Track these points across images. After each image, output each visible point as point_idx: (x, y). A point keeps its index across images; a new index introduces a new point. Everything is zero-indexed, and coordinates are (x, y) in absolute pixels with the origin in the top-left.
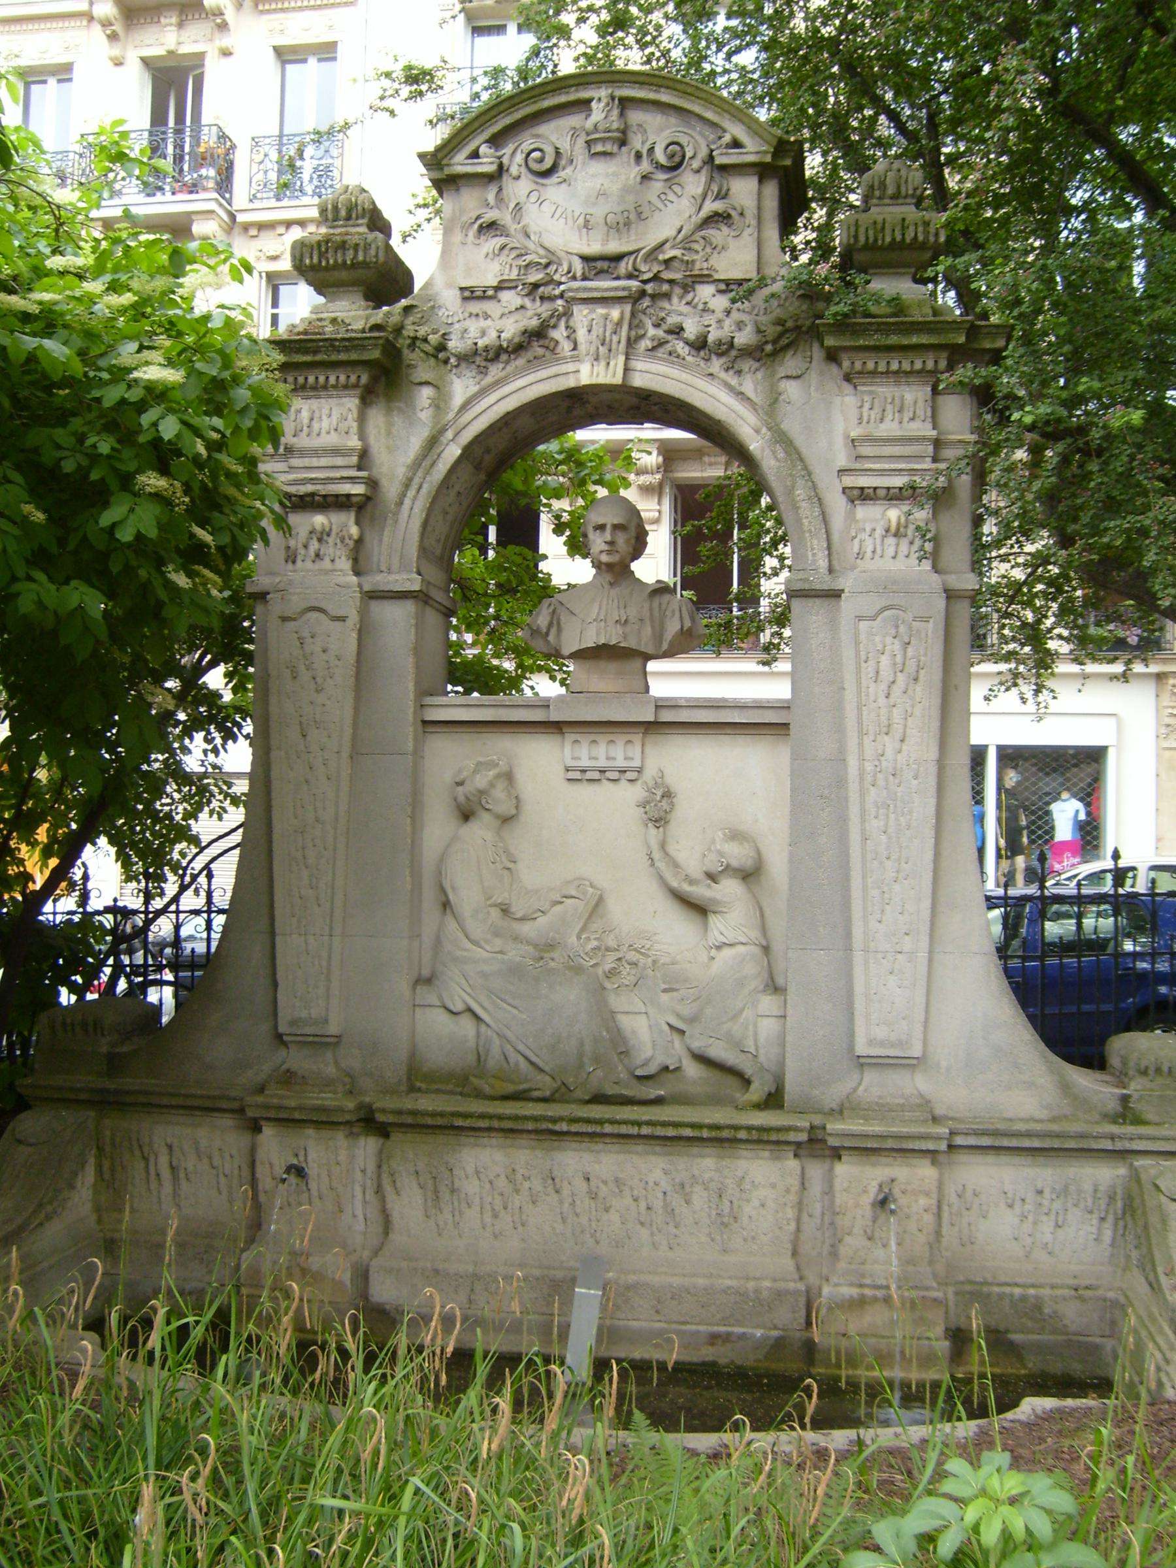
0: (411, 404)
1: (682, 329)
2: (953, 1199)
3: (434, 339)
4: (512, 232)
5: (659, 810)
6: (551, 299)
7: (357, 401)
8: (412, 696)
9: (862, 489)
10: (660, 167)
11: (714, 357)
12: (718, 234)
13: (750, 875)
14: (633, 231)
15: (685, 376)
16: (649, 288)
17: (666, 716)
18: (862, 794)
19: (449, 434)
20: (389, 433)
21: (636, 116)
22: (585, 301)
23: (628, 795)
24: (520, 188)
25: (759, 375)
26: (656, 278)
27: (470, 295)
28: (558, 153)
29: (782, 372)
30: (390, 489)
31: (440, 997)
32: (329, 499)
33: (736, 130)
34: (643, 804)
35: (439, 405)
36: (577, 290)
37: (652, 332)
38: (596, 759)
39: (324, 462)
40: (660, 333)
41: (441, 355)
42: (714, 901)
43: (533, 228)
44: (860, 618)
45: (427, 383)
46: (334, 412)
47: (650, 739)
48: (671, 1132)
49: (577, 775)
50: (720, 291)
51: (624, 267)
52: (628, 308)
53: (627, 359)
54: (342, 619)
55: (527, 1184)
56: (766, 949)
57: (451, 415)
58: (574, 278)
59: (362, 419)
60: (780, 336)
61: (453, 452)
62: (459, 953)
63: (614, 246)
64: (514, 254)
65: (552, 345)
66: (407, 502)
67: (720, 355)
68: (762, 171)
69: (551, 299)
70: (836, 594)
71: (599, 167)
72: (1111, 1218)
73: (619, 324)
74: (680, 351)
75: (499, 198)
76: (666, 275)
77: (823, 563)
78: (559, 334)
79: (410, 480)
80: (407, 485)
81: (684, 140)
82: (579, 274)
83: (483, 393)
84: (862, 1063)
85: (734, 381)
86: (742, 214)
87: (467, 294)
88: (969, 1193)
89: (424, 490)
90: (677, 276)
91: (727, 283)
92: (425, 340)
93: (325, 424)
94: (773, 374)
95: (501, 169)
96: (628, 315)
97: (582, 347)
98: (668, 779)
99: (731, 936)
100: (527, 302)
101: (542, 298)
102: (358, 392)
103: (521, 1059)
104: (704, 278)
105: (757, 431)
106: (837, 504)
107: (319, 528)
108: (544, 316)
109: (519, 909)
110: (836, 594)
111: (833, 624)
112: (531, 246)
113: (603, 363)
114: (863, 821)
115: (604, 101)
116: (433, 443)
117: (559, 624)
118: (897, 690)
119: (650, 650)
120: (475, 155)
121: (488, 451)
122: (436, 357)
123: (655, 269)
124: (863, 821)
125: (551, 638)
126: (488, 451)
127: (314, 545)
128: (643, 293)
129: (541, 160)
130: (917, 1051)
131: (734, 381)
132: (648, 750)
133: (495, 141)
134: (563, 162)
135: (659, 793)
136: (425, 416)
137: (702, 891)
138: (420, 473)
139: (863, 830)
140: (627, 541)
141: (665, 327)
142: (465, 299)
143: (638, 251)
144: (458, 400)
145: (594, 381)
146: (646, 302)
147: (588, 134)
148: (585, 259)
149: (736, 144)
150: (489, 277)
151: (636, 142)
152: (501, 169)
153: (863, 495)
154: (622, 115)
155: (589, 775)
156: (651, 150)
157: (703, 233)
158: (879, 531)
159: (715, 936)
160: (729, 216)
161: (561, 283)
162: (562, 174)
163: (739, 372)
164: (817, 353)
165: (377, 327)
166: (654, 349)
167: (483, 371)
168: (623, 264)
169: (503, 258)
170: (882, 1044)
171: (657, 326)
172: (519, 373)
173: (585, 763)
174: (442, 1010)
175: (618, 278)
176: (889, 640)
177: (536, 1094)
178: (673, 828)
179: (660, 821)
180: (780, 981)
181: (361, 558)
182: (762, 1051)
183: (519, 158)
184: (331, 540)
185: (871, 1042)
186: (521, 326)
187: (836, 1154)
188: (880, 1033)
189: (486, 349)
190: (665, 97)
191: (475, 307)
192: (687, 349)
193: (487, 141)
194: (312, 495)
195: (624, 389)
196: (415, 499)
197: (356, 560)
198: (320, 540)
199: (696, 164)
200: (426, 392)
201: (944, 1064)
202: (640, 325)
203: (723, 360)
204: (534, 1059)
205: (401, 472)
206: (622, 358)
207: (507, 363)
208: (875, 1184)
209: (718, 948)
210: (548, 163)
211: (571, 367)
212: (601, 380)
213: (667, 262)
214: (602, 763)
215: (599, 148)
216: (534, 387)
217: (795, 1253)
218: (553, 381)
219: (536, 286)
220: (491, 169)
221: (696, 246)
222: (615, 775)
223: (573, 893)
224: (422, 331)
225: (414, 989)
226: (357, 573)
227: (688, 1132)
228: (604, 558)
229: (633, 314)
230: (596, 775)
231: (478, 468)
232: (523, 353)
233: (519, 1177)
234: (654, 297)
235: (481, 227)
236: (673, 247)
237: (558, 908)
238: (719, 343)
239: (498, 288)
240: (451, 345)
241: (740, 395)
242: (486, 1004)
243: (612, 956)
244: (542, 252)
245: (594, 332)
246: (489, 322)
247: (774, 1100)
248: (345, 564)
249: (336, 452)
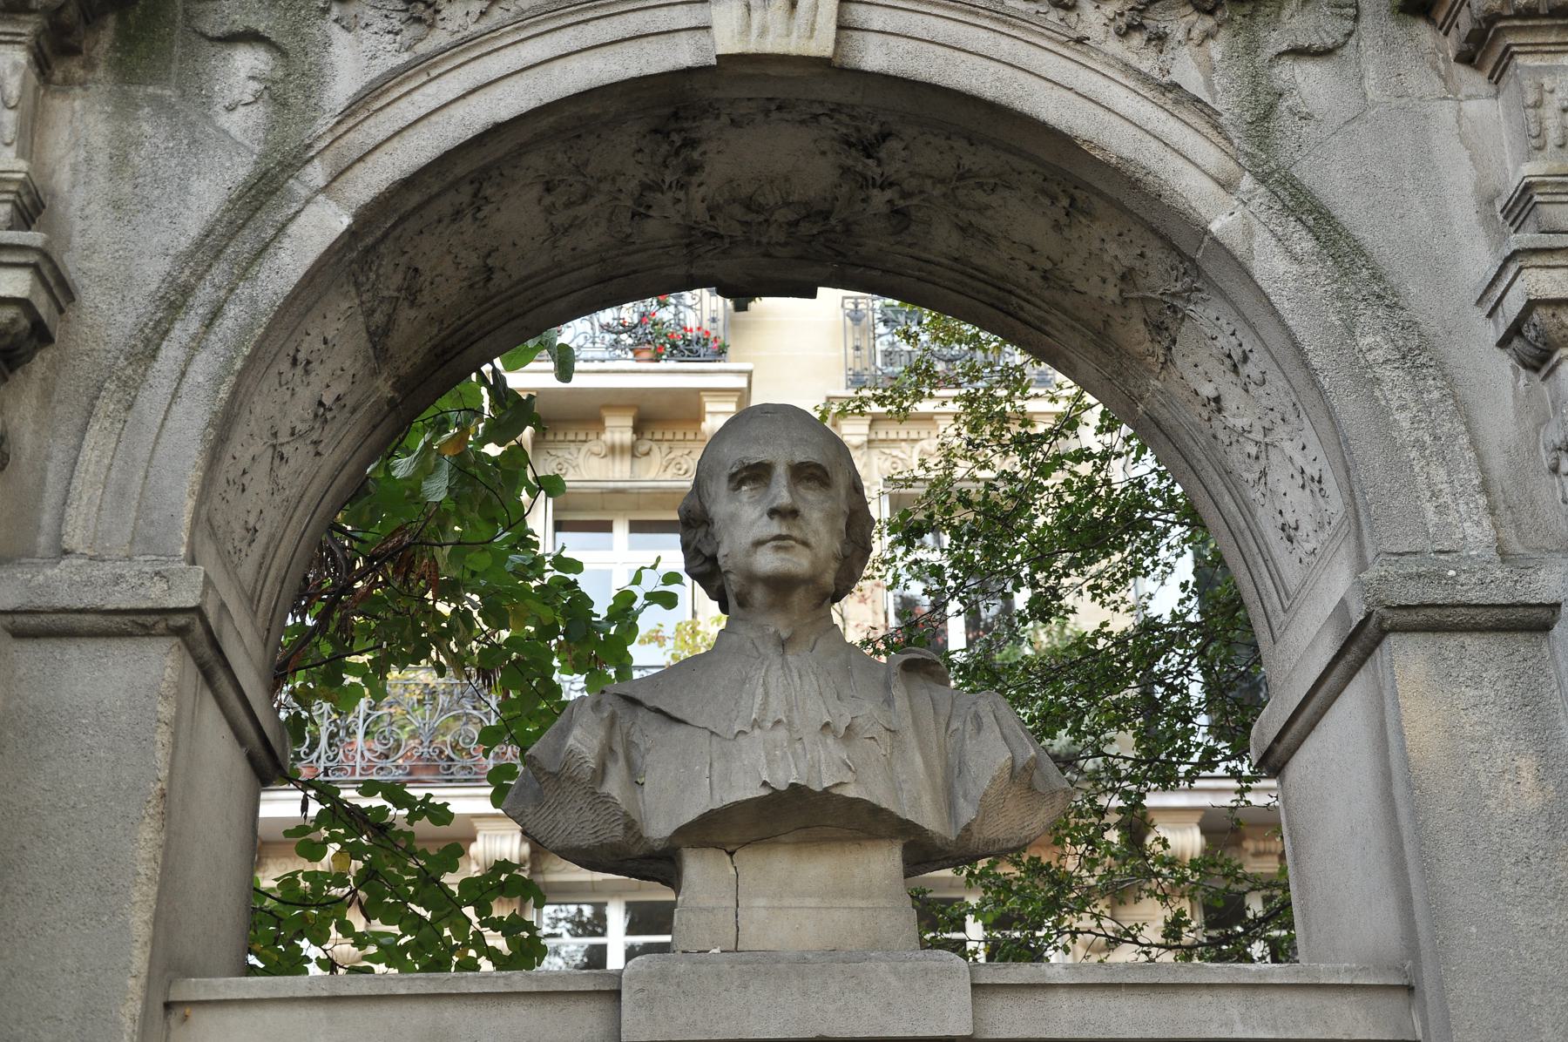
0: (198, 95)
7: (20, 56)
19: (316, 173)
20: (120, 162)
25: (1216, 49)
29: (1277, 41)
30: (108, 314)
35: (286, 95)
45: (251, 37)
57: (323, 124)
61: (321, 224)
66: (171, 353)
79: (187, 291)
80: (174, 301)
83: (422, 67)
85: (1148, 63)
94: (1252, 48)
105: (1227, 185)
110: (1533, 621)
116: (263, 193)
117: (629, 745)
125: (614, 786)
131: (1148, 63)
138: (219, 273)
140: (831, 518)
144: (343, 86)
145: (753, 46)
163: (1159, 39)
196: (199, 341)
200: (247, 62)
205: (154, 271)
216: (574, 63)
228: (768, 562)
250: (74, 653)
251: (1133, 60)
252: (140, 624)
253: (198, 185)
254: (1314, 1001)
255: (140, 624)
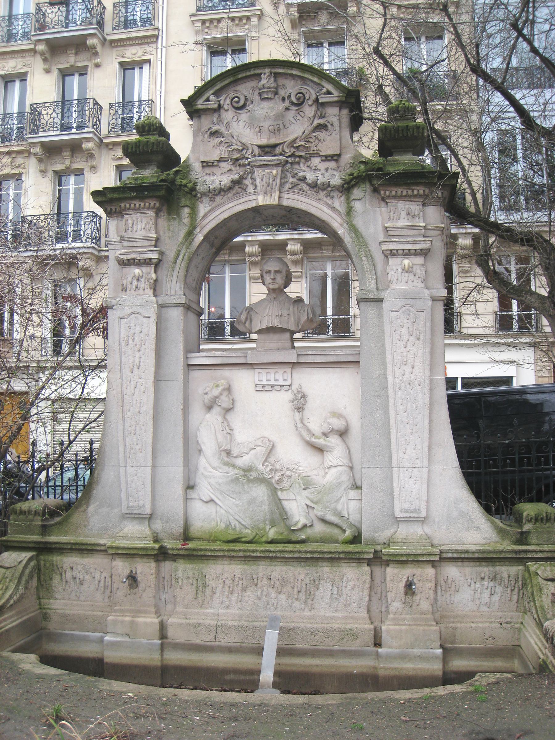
1: (305, 178)
2: (442, 583)
3: (190, 185)
4: (225, 135)
5: (300, 404)
6: (245, 165)
8: (182, 353)
9: (391, 250)
10: (293, 103)
11: (320, 191)
12: (322, 135)
13: (343, 433)
14: (281, 134)
15: (307, 200)
16: (289, 160)
17: (302, 360)
18: (395, 394)
19: (198, 230)
21: (281, 81)
22: (260, 166)
23: (285, 397)
24: (228, 115)
26: (293, 155)
27: (205, 164)
28: (246, 99)
31: (199, 495)
32: (142, 261)
33: (329, 87)
34: (292, 401)
36: (256, 161)
37: (291, 180)
38: (269, 380)
39: (139, 244)
40: (295, 180)
41: (194, 193)
42: (327, 446)
43: (235, 134)
44: (392, 311)
45: (187, 206)
46: (143, 220)
47: (295, 371)
48: (309, 556)
49: (261, 388)
50: (322, 161)
51: (278, 150)
52: (280, 169)
53: (280, 193)
54: (149, 317)
55: (241, 582)
56: (351, 468)
58: (255, 156)
59: (156, 224)
60: (351, 180)
61: (200, 238)
62: (206, 473)
63: (273, 141)
64: (226, 145)
65: (245, 187)
67: (323, 190)
68: (341, 104)
69: (245, 165)
70: (380, 300)
71: (265, 104)
72: (516, 590)
73: (276, 176)
74: (304, 188)
75: (220, 121)
76: (298, 154)
77: (374, 286)
78: (248, 182)
79: (180, 251)
81: (304, 91)
82: (257, 154)
84: (398, 521)
85: (330, 202)
86: (332, 125)
87: (205, 164)
88: (450, 581)
89: (186, 257)
90: (303, 154)
91: (326, 156)
92: (185, 186)
93: (139, 226)
95: (220, 107)
96: (280, 173)
97: (259, 188)
98: (304, 389)
99: (335, 462)
100: (232, 167)
101: (240, 165)
102: (154, 211)
103: (237, 523)
104: (316, 155)
105: (341, 225)
106: (379, 257)
107: (137, 275)
108: (241, 173)
109: (235, 452)
110: (380, 300)
111: (380, 314)
112: (234, 141)
113: (269, 195)
114: (395, 406)
115: (267, 74)
118: (409, 345)
119: (293, 329)
120: (208, 100)
121: (216, 238)
122: (190, 194)
123: (293, 150)
124: (395, 406)
125: (247, 324)
126: (216, 238)
127: (135, 283)
128: (287, 162)
129: (238, 102)
130: (424, 514)
131: (330, 202)
132: (294, 375)
133: (217, 94)
134: (248, 103)
135: (300, 396)
136: (186, 221)
137: (321, 442)
139: (396, 410)
140: (282, 278)
141: (297, 178)
142: (203, 167)
143: (284, 142)
146: (289, 166)
147: (260, 90)
148: (260, 147)
149: (329, 93)
150: (215, 157)
151: (282, 92)
152: (220, 107)
153: (393, 253)
154: (275, 81)
155: (266, 388)
156: (289, 96)
157: (314, 134)
158: (400, 270)
159: (328, 463)
160: (326, 126)
161: (248, 159)
162: (248, 108)
163: (332, 198)
164: (369, 188)
165: (162, 180)
166: (292, 188)
167: (212, 200)
168: (277, 149)
169: (221, 148)
170: (407, 511)
171: (293, 177)
172: (230, 200)
173: (264, 382)
174: (199, 501)
175: (275, 155)
176: (405, 321)
177: (244, 539)
178: (306, 413)
179: (300, 409)
180: (359, 483)
181: (157, 288)
182: (351, 516)
183: (228, 101)
184: (143, 280)
185: (402, 511)
186: (230, 179)
187: (387, 563)
188: (406, 506)
189: (214, 190)
190: (295, 72)
191: (208, 170)
192: (308, 187)
193: (213, 94)
194: (134, 259)
195: (279, 206)
197: (154, 290)
198: (138, 280)
199: (310, 102)
201: (437, 520)
202: (286, 177)
203: (325, 192)
204: (243, 523)
206: (277, 193)
207: (224, 196)
208: (405, 577)
209: (329, 468)
210: (241, 103)
211: (254, 197)
212: (268, 203)
213: (297, 148)
214: (273, 382)
215: (265, 96)
216: (237, 207)
217: (369, 611)
218: (246, 203)
219: (237, 160)
220: (216, 106)
221: (311, 140)
222: (279, 388)
223: (260, 444)
224: (184, 182)
225: (186, 491)
226: (155, 296)
227: (316, 555)
228: (271, 286)
229: (282, 172)
230: (270, 388)
231: (212, 246)
232: (231, 191)
233: (237, 579)
234: (292, 163)
235: (211, 133)
236: (300, 141)
237: (253, 451)
238: (323, 184)
239: (219, 161)
240: (198, 188)
241: (333, 208)
242: (220, 497)
243: (279, 474)
244: (239, 144)
245: (264, 181)
246: (215, 177)
247: (356, 539)
248: (150, 292)
249: (144, 239)
250: (169, 309)
251: (328, 201)
252: (177, 305)
253: (181, 232)
254: (346, 356)
255: (177, 305)
